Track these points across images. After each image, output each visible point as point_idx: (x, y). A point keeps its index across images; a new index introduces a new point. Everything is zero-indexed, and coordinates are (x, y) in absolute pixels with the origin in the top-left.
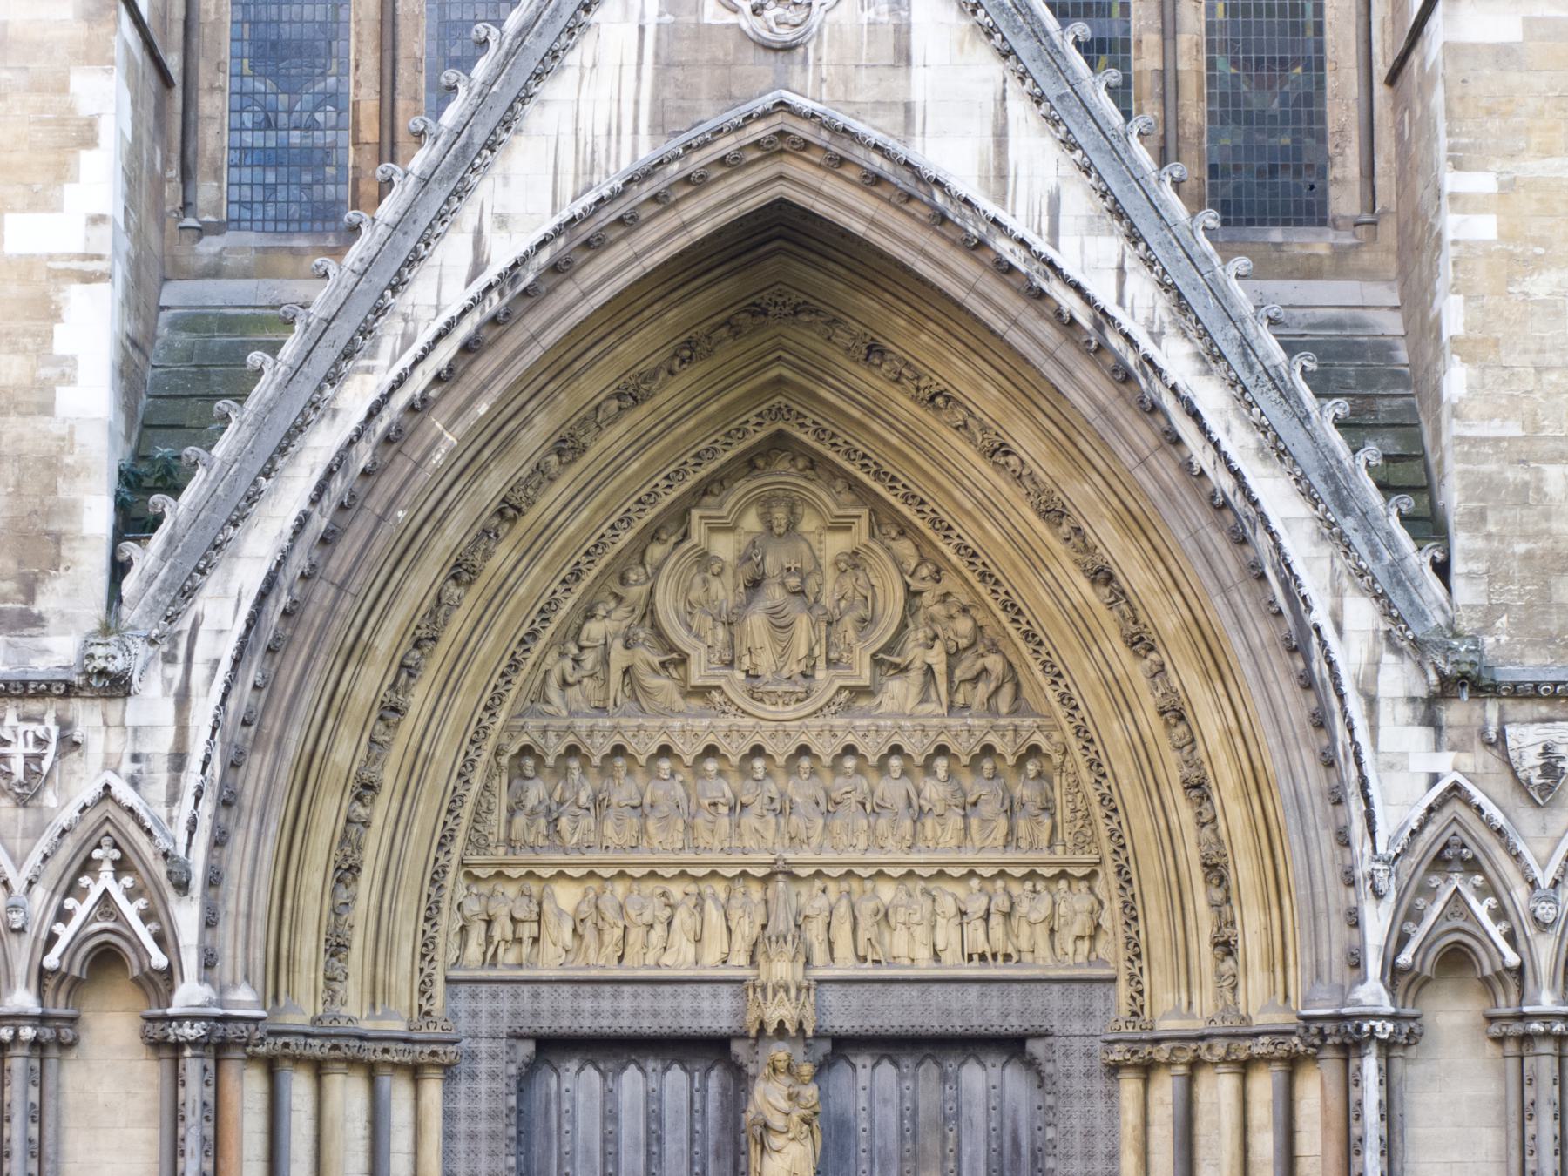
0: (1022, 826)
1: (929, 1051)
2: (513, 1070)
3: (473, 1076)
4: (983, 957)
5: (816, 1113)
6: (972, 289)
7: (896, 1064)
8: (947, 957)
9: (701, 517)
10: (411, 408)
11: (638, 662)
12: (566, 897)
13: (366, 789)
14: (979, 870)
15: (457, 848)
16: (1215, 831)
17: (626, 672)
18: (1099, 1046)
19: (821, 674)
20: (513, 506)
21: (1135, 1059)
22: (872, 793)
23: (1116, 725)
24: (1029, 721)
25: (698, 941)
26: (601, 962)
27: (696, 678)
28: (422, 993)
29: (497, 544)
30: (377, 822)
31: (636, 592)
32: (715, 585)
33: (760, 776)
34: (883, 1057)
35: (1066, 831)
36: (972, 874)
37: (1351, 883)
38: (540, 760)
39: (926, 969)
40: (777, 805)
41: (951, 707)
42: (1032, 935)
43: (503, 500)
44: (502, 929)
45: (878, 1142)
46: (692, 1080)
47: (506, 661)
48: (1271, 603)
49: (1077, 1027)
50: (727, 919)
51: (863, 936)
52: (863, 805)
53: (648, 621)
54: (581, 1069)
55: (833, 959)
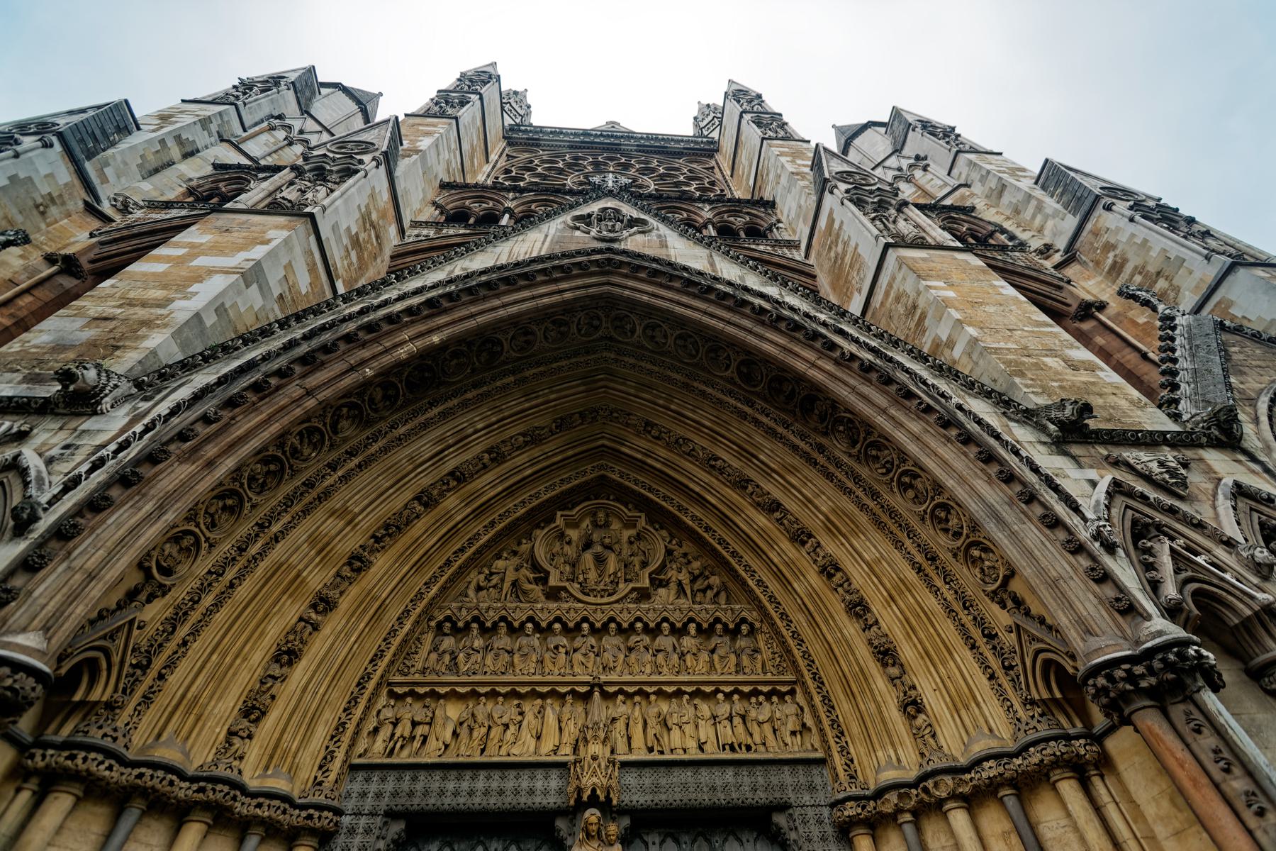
0: (745, 661)
1: (700, 829)
6: (705, 313)
8: (707, 747)
9: (562, 516)
10: (390, 319)
11: (521, 577)
12: (454, 711)
13: (324, 604)
14: (722, 688)
15: (383, 664)
16: (879, 628)
17: (515, 584)
18: (826, 812)
19: (621, 586)
21: (865, 813)
24: (738, 607)
25: (538, 738)
27: (553, 581)
28: (321, 767)
29: (449, 490)
30: (326, 630)
31: (525, 547)
32: (567, 548)
33: (585, 633)
36: (717, 691)
37: (1077, 548)
38: (454, 624)
39: (694, 754)
40: (596, 650)
41: (693, 603)
42: (762, 732)
44: (404, 729)
48: (920, 404)
49: (807, 798)
50: (560, 721)
51: (651, 732)
52: (648, 650)
55: (630, 750)
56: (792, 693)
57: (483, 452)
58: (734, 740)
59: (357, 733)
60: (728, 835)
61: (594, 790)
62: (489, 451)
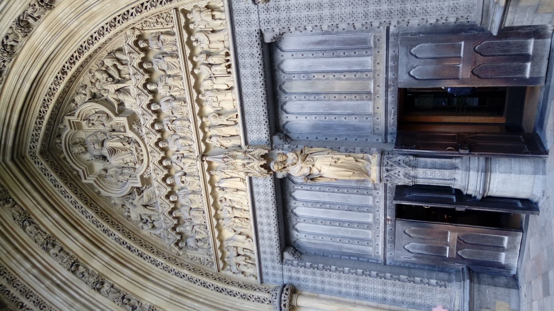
0: (167, 49)
2: (295, 262)
3: (298, 279)
4: (229, 66)
5: (302, 152)
7: (285, 103)
9: (85, 179)
11: (140, 203)
14: (190, 70)
17: (145, 206)
20: (71, 267)
22: (169, 116)
23: (95, 9)
25: (238, 190)
26: (250, 227)
29: (87, 270)
34: (282, 109)
35: (166, 26)
36: (193, 73)
42: (215, 42)
43: (69, 270)
45: (321, 111)
46: (298, 189)
47: (139, 258)
50: (227, 178)
52: (174, 120)
53: (128, 196)
54: (297, 230)
55: (237, 135)
56: (185, 12)
57: (49, 254)
58: (224, 65)
59: (246, 286)
60: (279, 69)
61: (261, 166)
62: (47, 250)
